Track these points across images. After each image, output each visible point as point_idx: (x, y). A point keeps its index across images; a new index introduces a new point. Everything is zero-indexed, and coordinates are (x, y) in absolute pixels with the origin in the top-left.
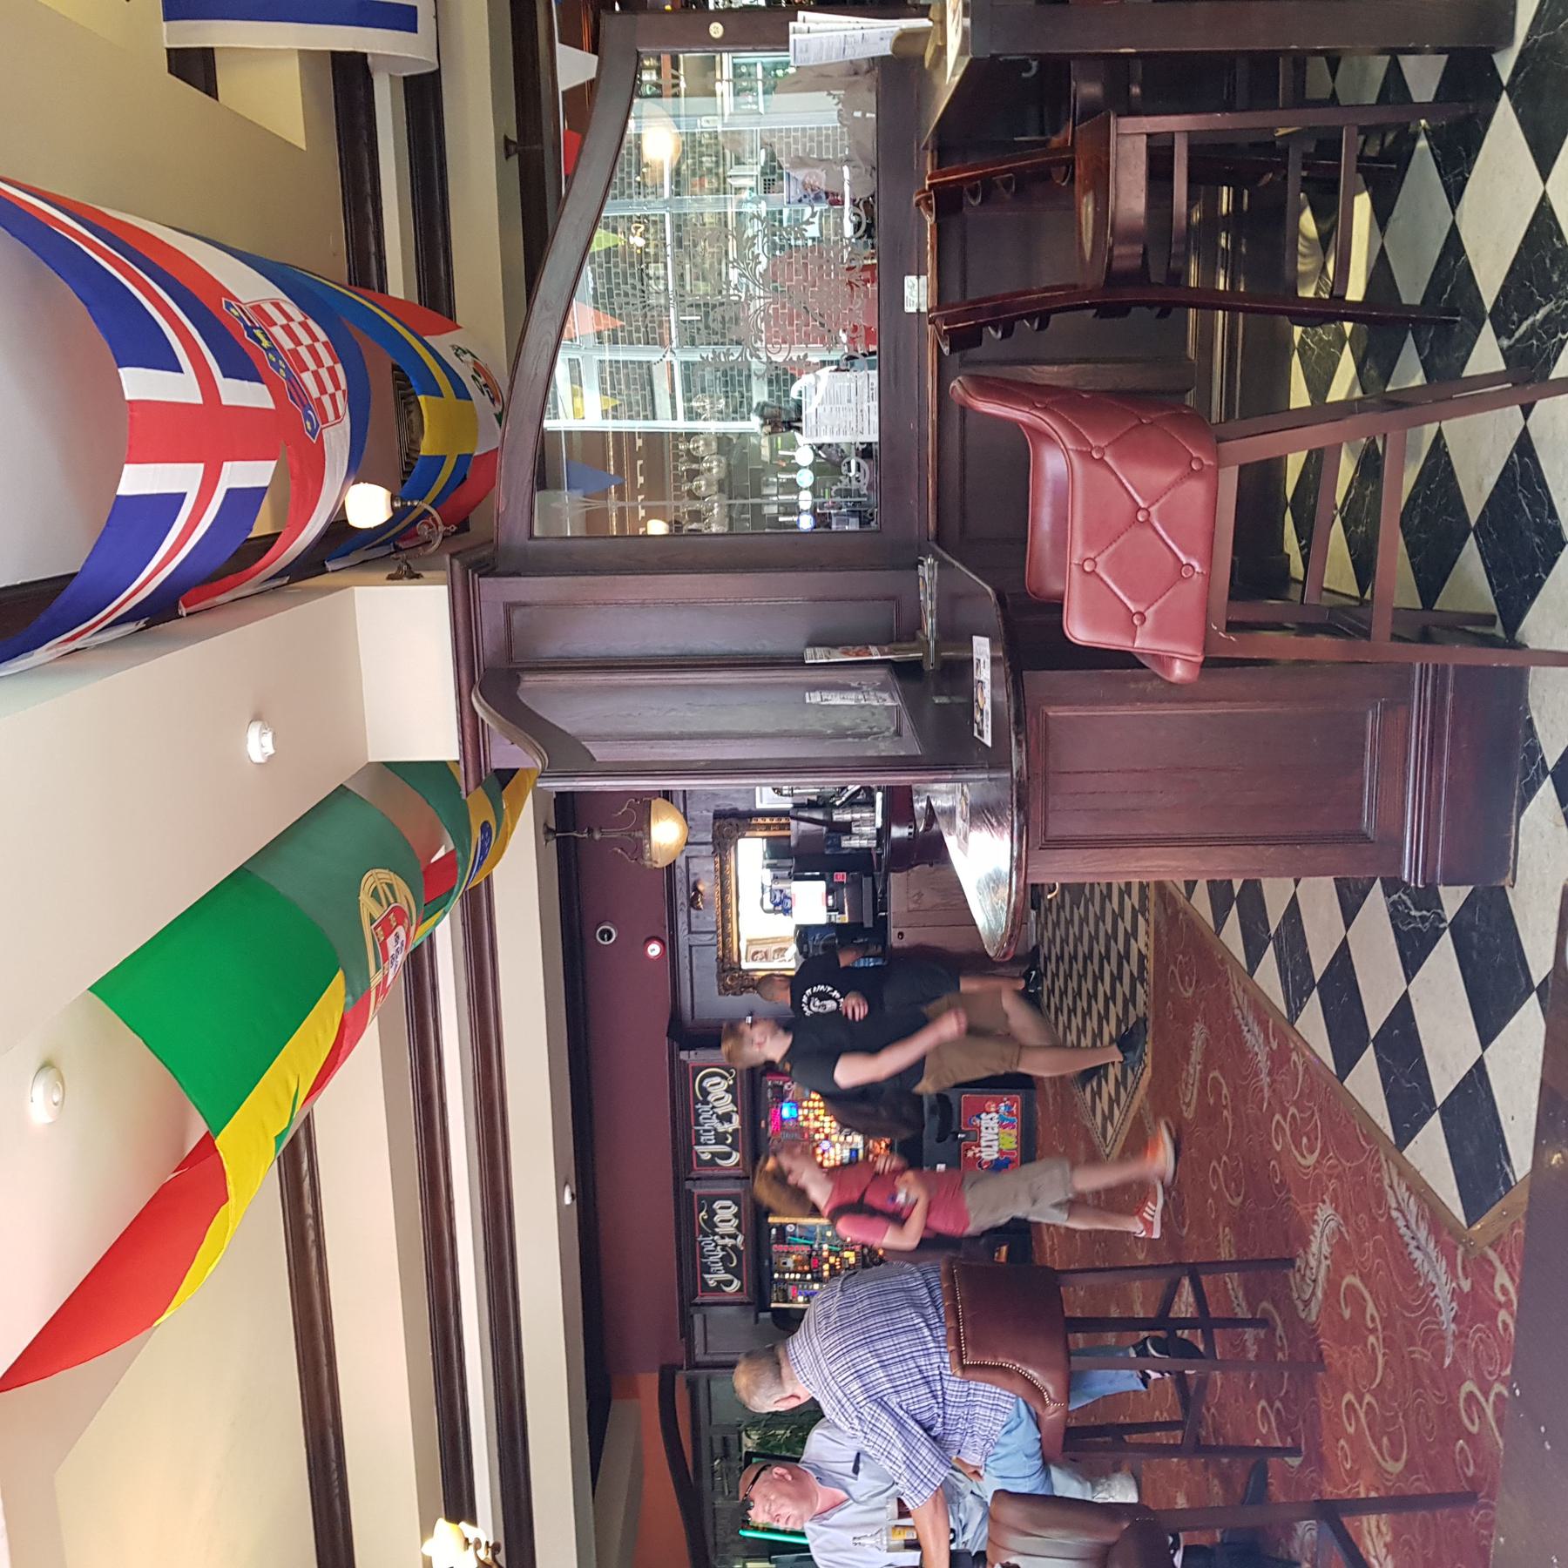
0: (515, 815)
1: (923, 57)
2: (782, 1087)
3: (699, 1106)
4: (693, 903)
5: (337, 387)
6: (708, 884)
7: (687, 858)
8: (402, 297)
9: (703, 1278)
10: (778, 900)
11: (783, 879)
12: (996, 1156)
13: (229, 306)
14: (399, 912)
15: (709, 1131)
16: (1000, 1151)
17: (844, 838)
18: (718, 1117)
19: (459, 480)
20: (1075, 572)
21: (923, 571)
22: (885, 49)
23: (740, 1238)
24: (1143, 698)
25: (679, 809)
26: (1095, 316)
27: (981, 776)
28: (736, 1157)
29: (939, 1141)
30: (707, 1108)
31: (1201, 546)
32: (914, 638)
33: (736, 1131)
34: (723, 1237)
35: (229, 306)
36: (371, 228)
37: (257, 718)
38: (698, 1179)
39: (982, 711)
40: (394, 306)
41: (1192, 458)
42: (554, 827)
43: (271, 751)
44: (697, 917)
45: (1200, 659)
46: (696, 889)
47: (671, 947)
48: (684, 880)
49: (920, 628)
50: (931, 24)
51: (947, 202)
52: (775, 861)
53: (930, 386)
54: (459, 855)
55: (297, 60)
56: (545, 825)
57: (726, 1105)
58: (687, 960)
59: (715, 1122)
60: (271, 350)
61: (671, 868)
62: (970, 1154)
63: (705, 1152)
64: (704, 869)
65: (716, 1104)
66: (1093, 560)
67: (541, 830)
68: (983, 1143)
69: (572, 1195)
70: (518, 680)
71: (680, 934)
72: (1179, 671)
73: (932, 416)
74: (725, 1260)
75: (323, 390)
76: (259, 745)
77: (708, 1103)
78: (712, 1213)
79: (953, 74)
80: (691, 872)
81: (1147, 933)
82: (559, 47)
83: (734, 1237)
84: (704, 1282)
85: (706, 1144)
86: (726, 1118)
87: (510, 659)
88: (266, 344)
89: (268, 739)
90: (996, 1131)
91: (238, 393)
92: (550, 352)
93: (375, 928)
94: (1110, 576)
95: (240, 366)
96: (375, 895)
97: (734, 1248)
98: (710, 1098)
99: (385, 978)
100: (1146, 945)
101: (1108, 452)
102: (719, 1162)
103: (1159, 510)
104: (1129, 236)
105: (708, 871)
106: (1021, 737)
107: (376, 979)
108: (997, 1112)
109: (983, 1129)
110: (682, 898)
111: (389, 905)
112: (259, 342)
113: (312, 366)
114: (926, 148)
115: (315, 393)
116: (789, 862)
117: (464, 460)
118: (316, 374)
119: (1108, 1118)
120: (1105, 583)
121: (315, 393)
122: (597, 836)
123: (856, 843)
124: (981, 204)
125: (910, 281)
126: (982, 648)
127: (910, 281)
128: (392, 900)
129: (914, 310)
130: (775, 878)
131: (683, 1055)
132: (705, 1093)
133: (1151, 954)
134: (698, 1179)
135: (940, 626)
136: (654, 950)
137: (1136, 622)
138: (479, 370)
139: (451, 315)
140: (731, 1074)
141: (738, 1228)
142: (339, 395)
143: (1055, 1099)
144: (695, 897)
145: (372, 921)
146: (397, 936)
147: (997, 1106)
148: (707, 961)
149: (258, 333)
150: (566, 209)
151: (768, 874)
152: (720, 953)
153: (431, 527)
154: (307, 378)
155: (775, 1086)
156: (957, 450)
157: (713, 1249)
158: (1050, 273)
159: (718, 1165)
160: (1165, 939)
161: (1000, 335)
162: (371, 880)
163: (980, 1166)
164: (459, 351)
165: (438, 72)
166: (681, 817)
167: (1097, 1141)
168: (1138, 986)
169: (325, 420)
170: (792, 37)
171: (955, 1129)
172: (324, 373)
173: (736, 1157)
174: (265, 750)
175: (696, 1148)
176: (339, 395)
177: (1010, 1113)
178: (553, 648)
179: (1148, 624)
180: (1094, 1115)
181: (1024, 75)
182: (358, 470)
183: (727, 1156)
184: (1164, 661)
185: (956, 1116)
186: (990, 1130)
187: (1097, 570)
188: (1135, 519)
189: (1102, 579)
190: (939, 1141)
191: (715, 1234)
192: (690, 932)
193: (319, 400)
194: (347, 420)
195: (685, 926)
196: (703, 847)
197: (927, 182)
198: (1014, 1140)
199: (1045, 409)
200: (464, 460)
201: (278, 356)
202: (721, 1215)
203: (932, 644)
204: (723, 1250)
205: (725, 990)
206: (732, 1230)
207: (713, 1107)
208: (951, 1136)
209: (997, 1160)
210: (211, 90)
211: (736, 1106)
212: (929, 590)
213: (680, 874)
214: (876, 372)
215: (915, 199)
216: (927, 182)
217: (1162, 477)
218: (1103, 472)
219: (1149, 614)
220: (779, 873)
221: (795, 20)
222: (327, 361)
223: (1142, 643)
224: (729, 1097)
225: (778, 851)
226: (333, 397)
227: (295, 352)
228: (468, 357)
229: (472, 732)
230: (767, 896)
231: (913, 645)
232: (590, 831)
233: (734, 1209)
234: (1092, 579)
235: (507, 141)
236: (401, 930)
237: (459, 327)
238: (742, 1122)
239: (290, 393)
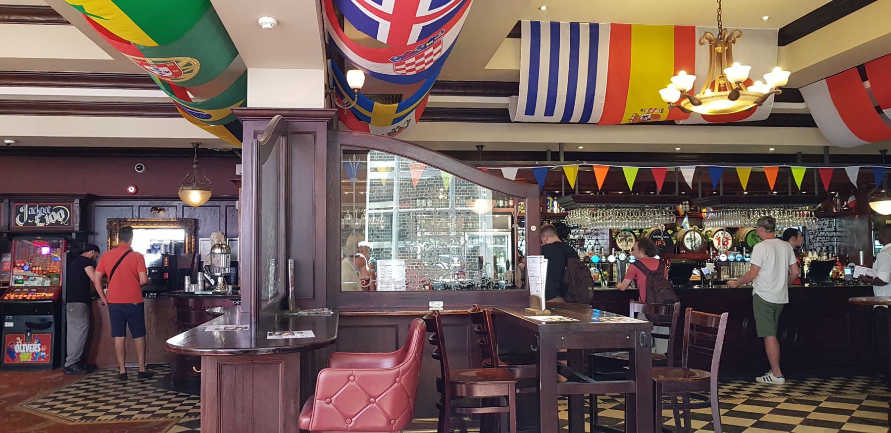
0: (211, 131)
1: (529, 307)
2: (59, 247)
3: (49, 207)
4: (155, 208)
5: (407, 71)
6: (163, 215)
7: (176, 206)
8: (428, 101)
10: (155, 247)
11: (166, 249)
13: (443, 32)
14: (180, 74)
15: (36, 212)
16: (19, 354)
17: (189, 277)
18: (43, 217)
19: (360, 117)
20: (350, 372)
21: (326, 310)
22: (533, 292)
24: (287, 408)
25: (205, 203)
26: (437, 378)
27: (253, 335)
28: (20, 224)
29: (26, 323)
30: (48, 211)
31: (358, 426)
32: (297, 306)
35: (443, 32)
36: (454, 91)
37: (278, 22)
38: (9, 206)
39: (281, 335)
40: (427, 97)
41: (395, 420)
42: (199, 147)
43: (263, 27)
44: (147, 210)
45: (310, 429)
46: (160, 210)
47: (132, 197)
48: (165, 205)
49: (301, 309)
50: (543, 310)
51: (478, 318)
52: (173, 246)
53: (402, 312)
54: (192, 103)
55: (516, 69)
56: (201, 143)
57: (49, 220)
58: (125, 204)
59: (40, 215)
60: (425, 46)
61: (178, 199)
62: (18, 339)
63: (24, 209)
64: (171, 214)
65: (50, 215)
66: (354, 380)
67: (199, 141)
68: (24, 345)
69: (9, 144)
70: (284, 135)
71: (139, 202)
72: (304, 420)
73: (391, 313)
75: (407, 65)
76: (267, 22)
77: (51, 211)
79: (527, 319)
80: (170, 208)
81: (143, 418)
82: (517, 168)
85: (28, 210)
86: (42, 220)
87: (292, 133)
88: (428, 44)
89: (269, 26)
90: (30, 351)
91: (416, 30)
92: (415, 158)
93: (173, 63)
94: (347, 387)
95: (426, 33)
96: (189, 64)
98: (53, 213)
99: (149, 65)
100: (137, 418)
101: (399, 384)
102: (19, 216)
103: (375, 407)
104: (470, 391)
105: (169, 215)
106: (277, 351)
107: (149, 60)
108: (41, 351)
109: (32, 345)
110: (157, 203)
111: (183, 70)
112: (429, 42)
113: (417, 62)
114: (494, 309)
115: (407, 62)
116: (173, 252)
117: (368, 120)
118: (413, 63)
119: (43, 405)
120: (344, 386)
121: (407, 62)
122: (195, 166)
123: (187, 282)
124: (477, 331)
125: (441, 304)
126: (309, 334)
127: (441, 304)
128: (185, 71)
129: (430, 305)
130: (166, 246)
131: (77, 201)
132: (57, 211)
133: (132, 420)
134: (9, 206)
135: (302, 317)
136: (132, 190)
137: (327, 400)
138: (401, 129)
139: (421, 120)
142: (404, 72)
143: (48, 379)
144: (158, 210)
145: (177, 62)
146: (168, 72)
147: (44, 351)
148: (126, 214)
149: (432, 42)
150: (469, 167)
151: (168, 243)
152: (129, 220)
153: (346, 104)
154: (413, 60)
155: (59, 244)
156: (374, 324)
158: (451, 360)
159: (16, 216)
160: (141, 427)
161: (431, 339)
162: (195, 63)
163: (11, 344)
164: (409, 121)
165: (510, 121)
166: (202, 204)
167: (29, 400)
168: (115, 416)
169: (396, 65)
170: (539, 256)
171: (33, 331)
172: (414, 66)
173: (20, 224)
174: (264, 24)
175: (27, 205)
176: (404, 72)
177: (40, 358)
178: (296, 152)
179: (327, 406)
180: (43, 398)
181: (532, 346)
182: (371, 76)
183: (22, 220)
184: (310, 413)
185: (39, 331)
186: (31, 348)
187: (350, 382)
188: (370, 399)
189: (346, 384)
190: (26, 323)
192: (139, 206)
193: (404, 63)
194: (394, 74)
195: (143, 204)
196: (181, 214)
197: (486, 309)
198: (25, 360)
199: (415, 358)
200: (368, 120)
201: (422, 49)
203: (296, 314)
205: (110, 222)
207: (48, 214)
208: (28, 329)
209: (14, 352)
210: (510, 36)
211: (49, 225)
212: (319, 312)
213: (168, 203)
214: (405, 290)
215: (476, 305)
216: (486, 309)
217: (387, 408)
218: (390, 382)
219: (331, 406)
220: (168, 247)
221: (545, 258)
222: (418, 68)
223: (318, 403)
224: (53, 222)
225: (179, 247)
226: (404, 69)
227: (423, 55)
228: (406, 125)
229: (264, 114)
230: (158, 242)
231: (294, 306)
232: (197, 163)
234: (345, 381)
235: (482, 146)
236: (170, 74)
237: (416, 122)
238: (39, 227)
239: (410, 52)
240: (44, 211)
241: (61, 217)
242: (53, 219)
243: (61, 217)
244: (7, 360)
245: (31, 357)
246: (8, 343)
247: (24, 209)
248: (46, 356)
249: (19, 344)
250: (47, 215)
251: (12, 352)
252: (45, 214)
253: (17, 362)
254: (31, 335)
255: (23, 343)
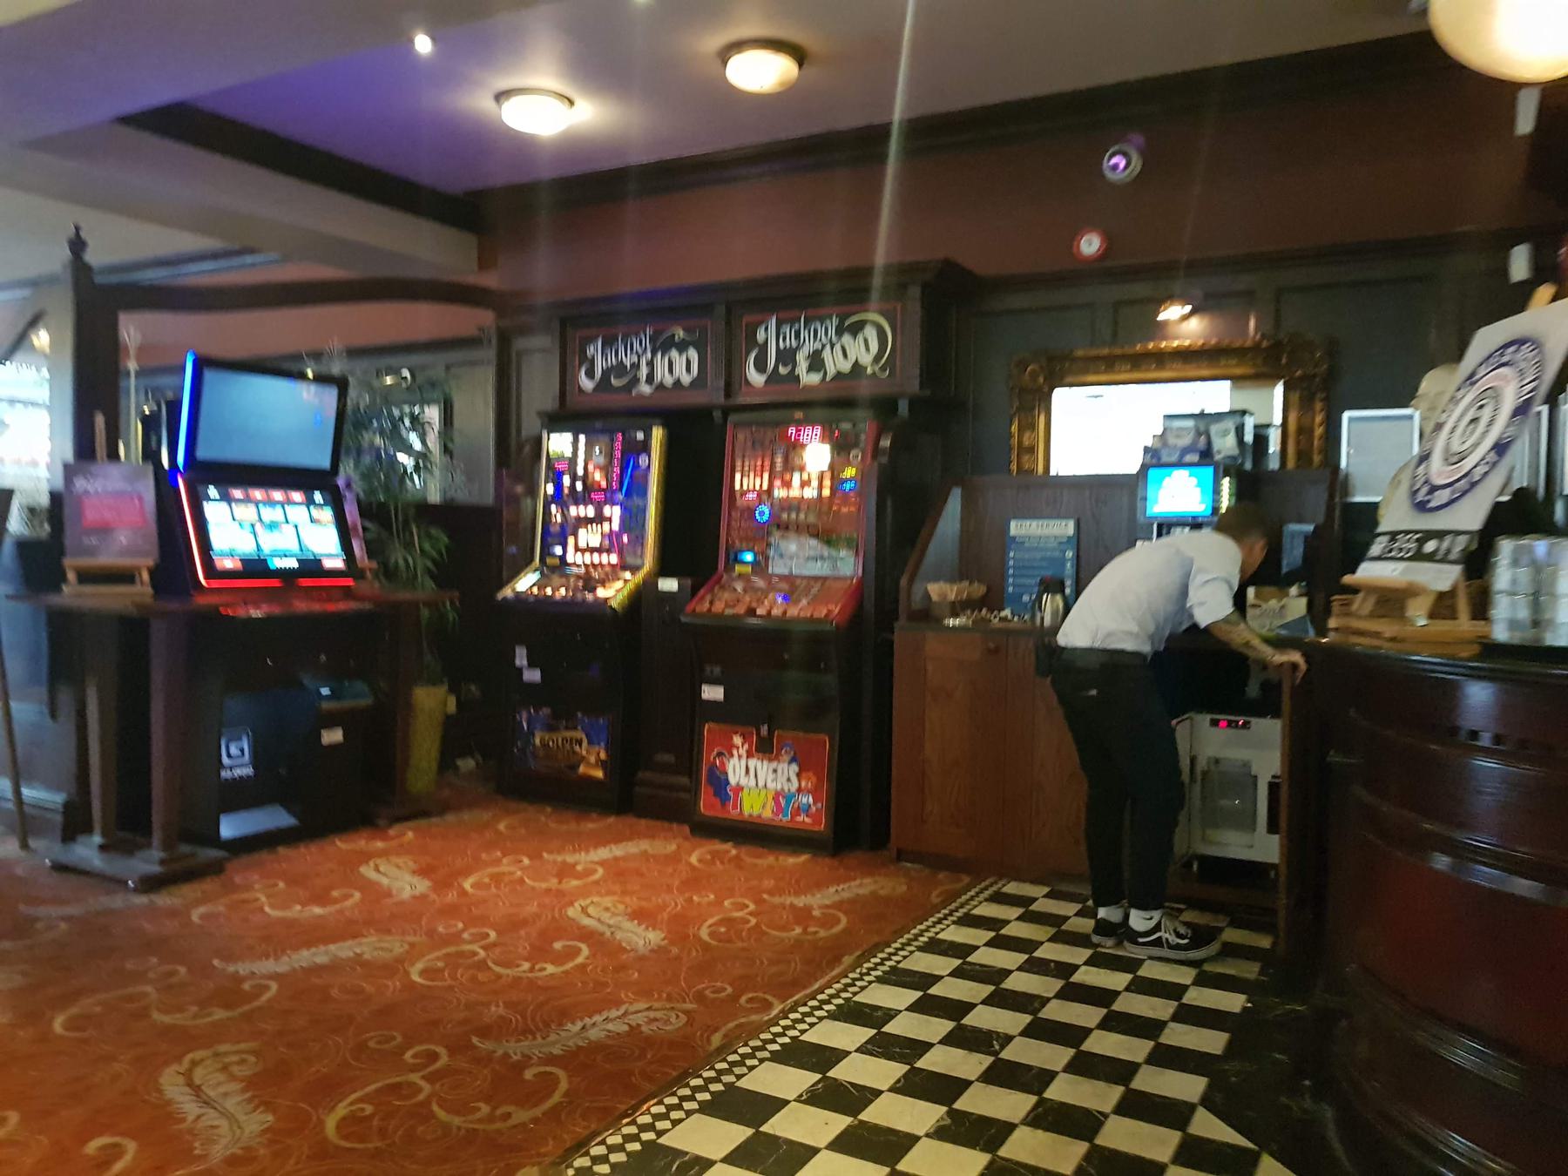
9: (596, 338)
12: (733, 781)
16: (739, 789)
23: (645, 389)
30: (832, 332)
33: (797, 379)
34: (651, 364)
57: (835, 363)
59: (809, 347)
62: (737, 740)
63: (768, 334)
65: (838, 348)
68: (753, 763)
74: (620, 369)
77: (840, 332)
78: (682, 347)
83: (650, 378)
84: (592, 339)
86: (816, 362)
90: (771, 785)
97: (636, 380)
98: (847, 339)
108: (799, 790)
109: (774, 765)
132: (856, 329)
136: (1090, 245)
140: (883, 369)
141: (661, 386)
155: (857, 436)
157: (635, 353)
163: (720, 754)
177: (797, 811)
183: (761, 366)
191: (654, 353)
192: (1118, 305)
198: (756, 812)
202: (679, 361)
204: (633, 365)
206: (658, 377)
209: (728, 782)
224: (846, 366)
233: (686, 380)
240: (821, 332)
241: (867, 349)
242: (845, 355)
243: (867, 349)
244: (706, 805)
245: (771, 804)
246: (709, 753)
247: (766, 329)
248: (814, 809)
249: (740, 757)
250: (828, 347)
251: (719, 783)
252: (824, 346)
253: (733, 813)
254: (771, 732)
255: (749, 755)
